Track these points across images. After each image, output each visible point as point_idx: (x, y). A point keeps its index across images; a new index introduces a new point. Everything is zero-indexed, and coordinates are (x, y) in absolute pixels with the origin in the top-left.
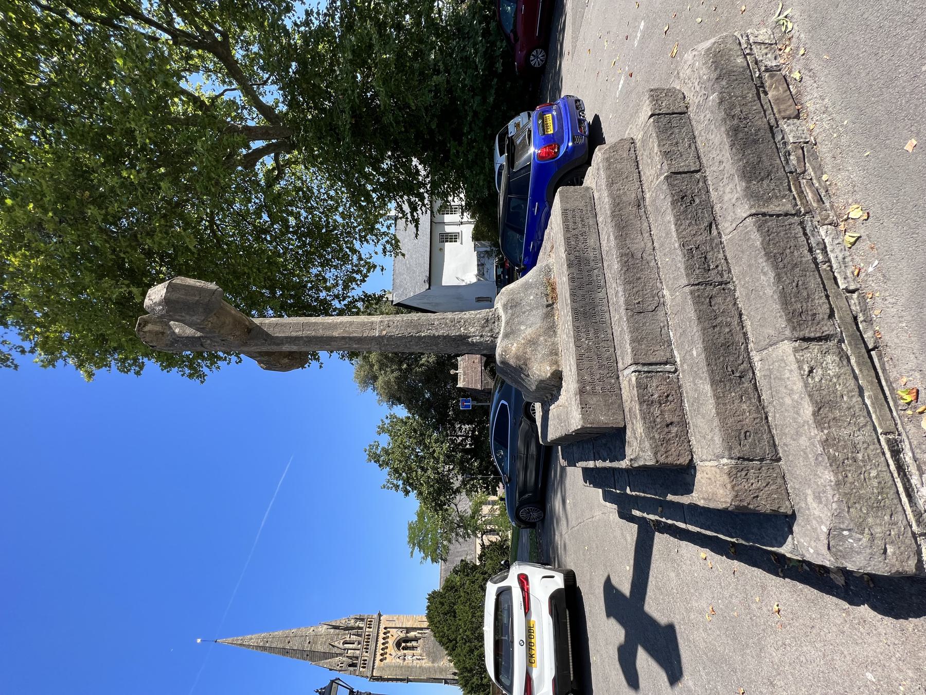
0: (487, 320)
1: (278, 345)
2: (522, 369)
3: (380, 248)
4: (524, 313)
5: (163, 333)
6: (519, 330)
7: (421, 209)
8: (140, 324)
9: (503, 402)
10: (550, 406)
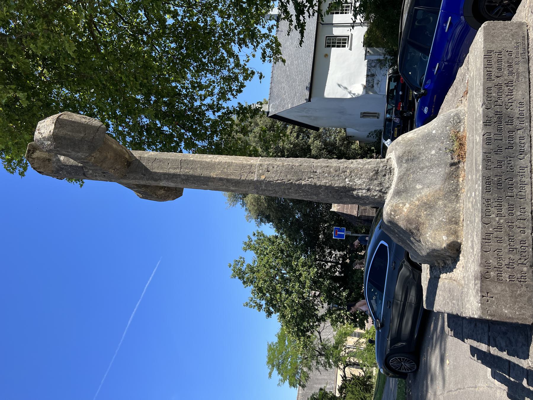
0: (377, 173)
1: (156, 180)
2: (412, 233)
4: (422, 169)
5: (49, 160)
6: (414, 188)
7: (308, 11)
8: (29, 151)
9: (382, 242)
10: (441, 273)
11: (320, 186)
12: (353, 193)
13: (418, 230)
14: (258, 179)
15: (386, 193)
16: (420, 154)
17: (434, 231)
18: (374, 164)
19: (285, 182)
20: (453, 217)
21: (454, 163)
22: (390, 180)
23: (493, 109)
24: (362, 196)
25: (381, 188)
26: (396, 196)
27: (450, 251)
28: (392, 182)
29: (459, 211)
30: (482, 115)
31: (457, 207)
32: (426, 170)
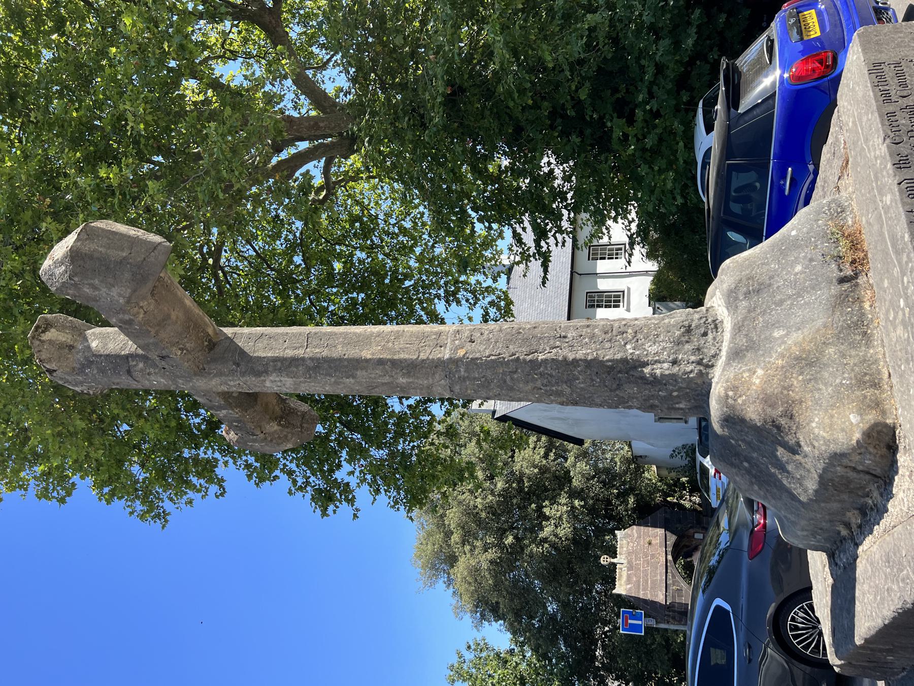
0: (689, 330)
1: (258, 374)
2: (779, 427)
3: (478, 313)
4: (781, 302)
5: (71, 347)
6: (769, 339)
7: (554, 236)
8: (37, 327)
9: (718, 602)
10: (857, 545)
11: (575, 362)
12: (643, 371)
13: (791, 417)
14: (453, 356)
15: (713, 366)
16: (771, 278)
17: (826, 411)
18: (681, 316)
19: (504, 358)
20: (866, 374)
21: (845, 277)
22: (717, 342)
23: (907, 142)
24: (662, 375)
25: (701, 357)
26: (734, 361)
27: (871, 450)
28: (721, 346)
29: (876, 361)
30: (887, 154)
31: (869, 355)
32: (789, 302)
